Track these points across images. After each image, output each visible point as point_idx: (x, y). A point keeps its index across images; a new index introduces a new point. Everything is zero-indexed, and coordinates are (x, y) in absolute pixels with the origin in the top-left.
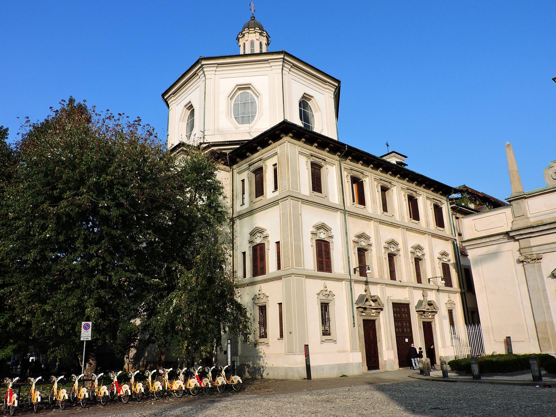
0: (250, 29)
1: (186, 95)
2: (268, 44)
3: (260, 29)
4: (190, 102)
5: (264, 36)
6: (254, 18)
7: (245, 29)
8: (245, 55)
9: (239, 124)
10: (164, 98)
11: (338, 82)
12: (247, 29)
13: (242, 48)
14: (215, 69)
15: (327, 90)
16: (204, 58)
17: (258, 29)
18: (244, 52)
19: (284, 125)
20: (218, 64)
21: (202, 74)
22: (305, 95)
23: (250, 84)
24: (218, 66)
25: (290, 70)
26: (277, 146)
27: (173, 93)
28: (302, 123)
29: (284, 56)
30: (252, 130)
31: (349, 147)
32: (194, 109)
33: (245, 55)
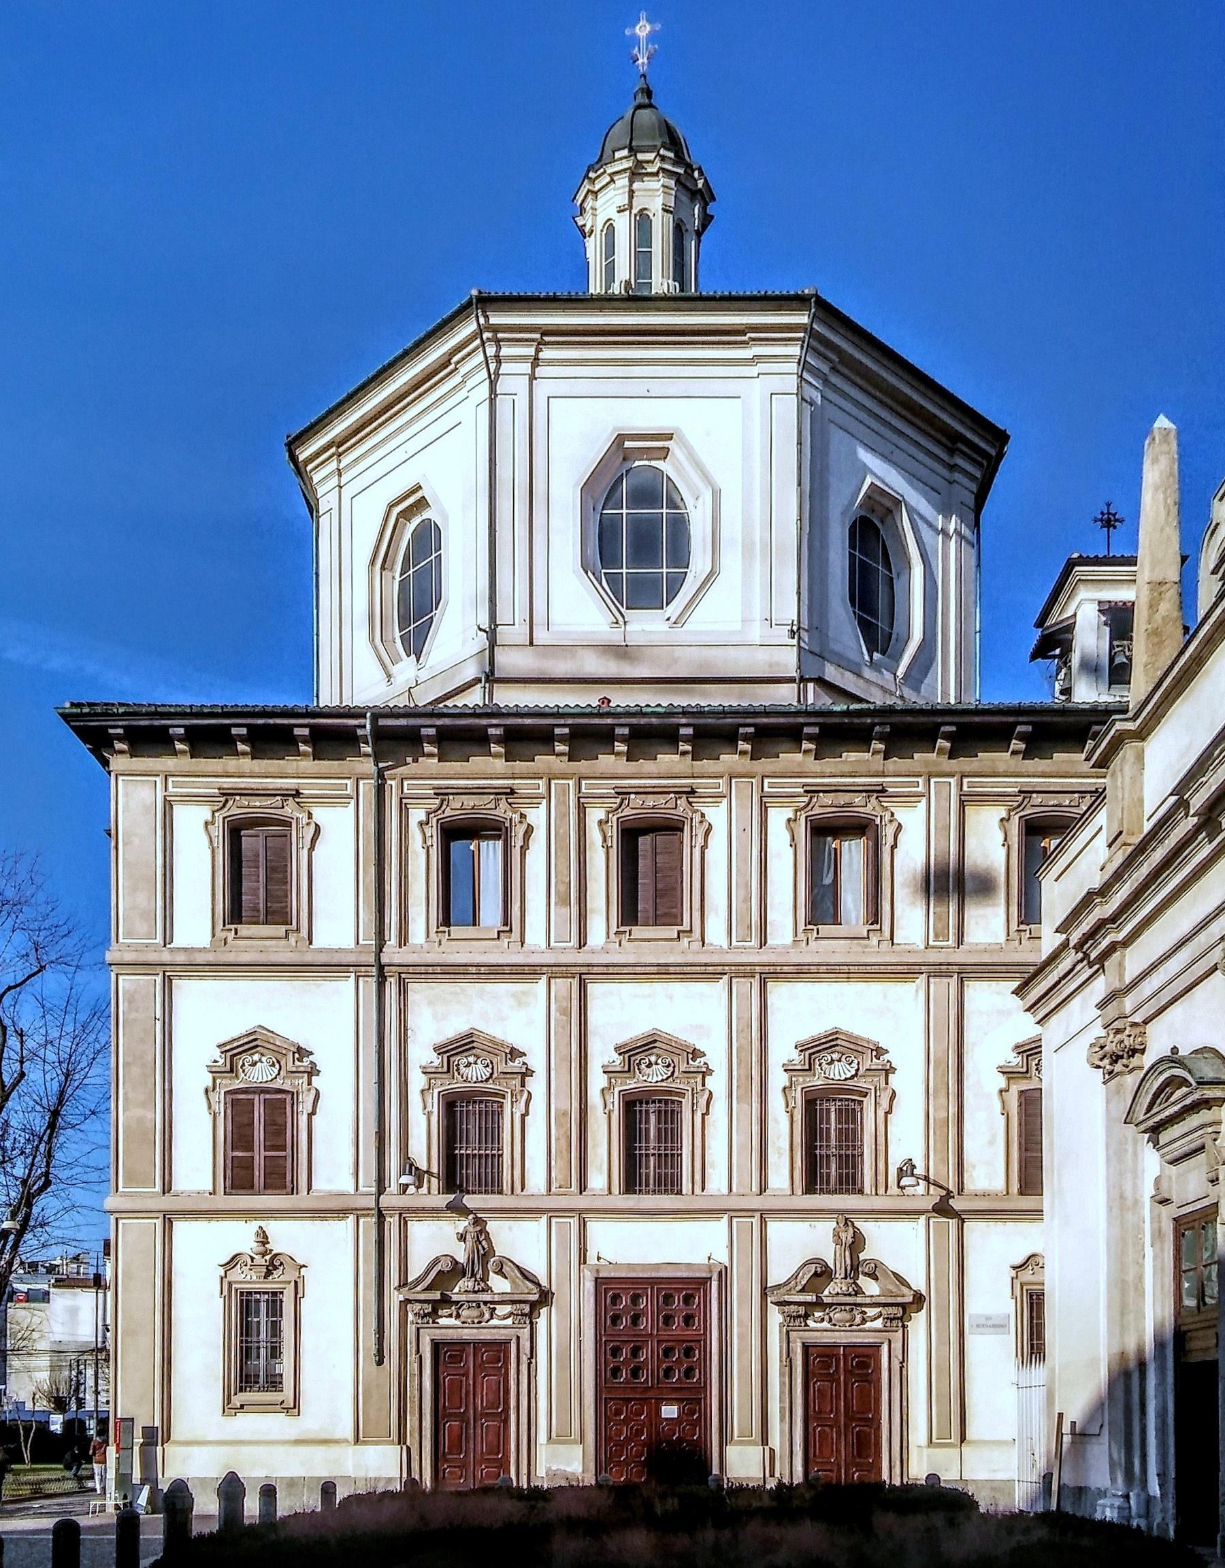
0: (640, 157)
3: (675, 163)
6: (649, 93)
7: (618, 155)
12: (625, 152)
14: (531, 351)
20: (546, 331)
24: (547, 339)
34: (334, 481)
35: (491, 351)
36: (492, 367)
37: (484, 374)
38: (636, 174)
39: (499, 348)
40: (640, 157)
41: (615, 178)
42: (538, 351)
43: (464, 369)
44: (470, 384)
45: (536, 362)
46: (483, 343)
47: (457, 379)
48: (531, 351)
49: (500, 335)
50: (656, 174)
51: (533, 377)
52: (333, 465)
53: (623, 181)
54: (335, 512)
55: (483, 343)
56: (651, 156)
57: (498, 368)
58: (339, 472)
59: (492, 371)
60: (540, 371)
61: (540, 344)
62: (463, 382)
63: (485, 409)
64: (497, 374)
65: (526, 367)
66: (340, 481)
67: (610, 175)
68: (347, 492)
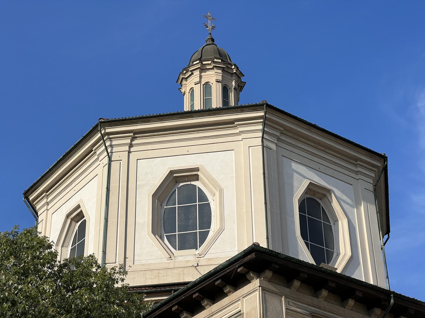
0: (204, 63)
1: (73, 192)
2: (240, 87)
4: (78, 207)
5: (232, 74)
6: (213, 40)
7: (194, 63)
8: (192, 114)
9: (176, 249)
10: (28, 200)
11: (384, 158)
12: (198, 62)
13: (187, 98)
15: (359, 176)
16: (108, 122)
17: (220, 61)
18: (192, 105)
19: (253, 255)
20: (136, 132)
21: (103, 151)
22: (312, 187)
23: (197, 169)
25: (279, 139)
26: (241, 298)
27: (47, 190)
28: (307, 244)
29: (266, 113)
30: (202, 262)
31: (398, 297)
32: (85, 220)
33: (192, 114)
34: (45, 208)
35: (108, 144)
36: (109, 150)
37: (106, 153)
38: (203, 69)
39: (111, 141)
40: (204, 63)
41: (193, 72)
42: (132, 141)
43: (98, 153)
44: (101, 158)
45: (131, 146)
46: (104, 141)
47: (96, 157)
48: (128, 141)
49: (111, 136)
50: (213, 69)
51: (129, 152)
52: (44, 201)
53: (197, 73)
54: (44, 221)
55: (104, 141)
56: (210, 62)
57: (112, 150)
58: (48, 203)
59: (109, 151)
60: (132, 149)
61: (133, 138)
62: (98, 158)
63: (107, 167)
64: (112, 152)
65: (127, 148)
66: (47, 207)
67: (191, 71)
68: (50, 212)
